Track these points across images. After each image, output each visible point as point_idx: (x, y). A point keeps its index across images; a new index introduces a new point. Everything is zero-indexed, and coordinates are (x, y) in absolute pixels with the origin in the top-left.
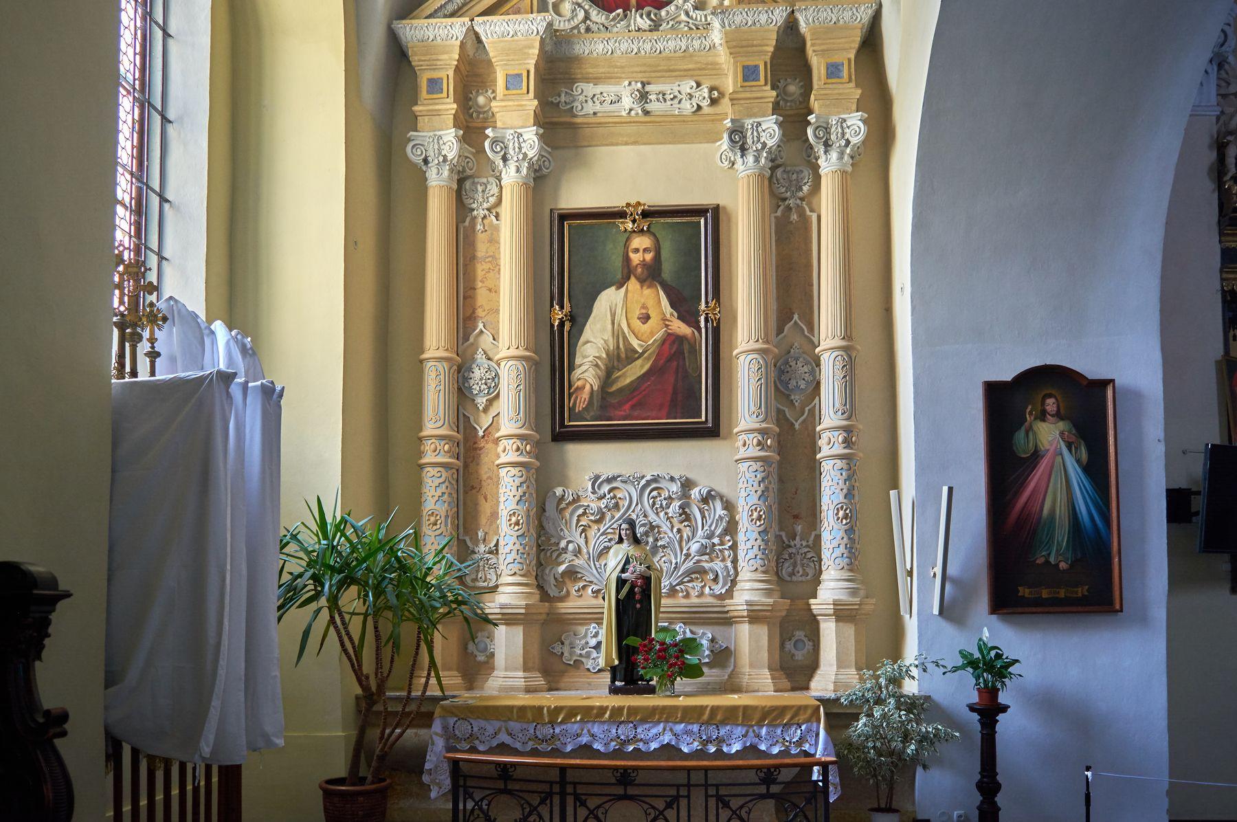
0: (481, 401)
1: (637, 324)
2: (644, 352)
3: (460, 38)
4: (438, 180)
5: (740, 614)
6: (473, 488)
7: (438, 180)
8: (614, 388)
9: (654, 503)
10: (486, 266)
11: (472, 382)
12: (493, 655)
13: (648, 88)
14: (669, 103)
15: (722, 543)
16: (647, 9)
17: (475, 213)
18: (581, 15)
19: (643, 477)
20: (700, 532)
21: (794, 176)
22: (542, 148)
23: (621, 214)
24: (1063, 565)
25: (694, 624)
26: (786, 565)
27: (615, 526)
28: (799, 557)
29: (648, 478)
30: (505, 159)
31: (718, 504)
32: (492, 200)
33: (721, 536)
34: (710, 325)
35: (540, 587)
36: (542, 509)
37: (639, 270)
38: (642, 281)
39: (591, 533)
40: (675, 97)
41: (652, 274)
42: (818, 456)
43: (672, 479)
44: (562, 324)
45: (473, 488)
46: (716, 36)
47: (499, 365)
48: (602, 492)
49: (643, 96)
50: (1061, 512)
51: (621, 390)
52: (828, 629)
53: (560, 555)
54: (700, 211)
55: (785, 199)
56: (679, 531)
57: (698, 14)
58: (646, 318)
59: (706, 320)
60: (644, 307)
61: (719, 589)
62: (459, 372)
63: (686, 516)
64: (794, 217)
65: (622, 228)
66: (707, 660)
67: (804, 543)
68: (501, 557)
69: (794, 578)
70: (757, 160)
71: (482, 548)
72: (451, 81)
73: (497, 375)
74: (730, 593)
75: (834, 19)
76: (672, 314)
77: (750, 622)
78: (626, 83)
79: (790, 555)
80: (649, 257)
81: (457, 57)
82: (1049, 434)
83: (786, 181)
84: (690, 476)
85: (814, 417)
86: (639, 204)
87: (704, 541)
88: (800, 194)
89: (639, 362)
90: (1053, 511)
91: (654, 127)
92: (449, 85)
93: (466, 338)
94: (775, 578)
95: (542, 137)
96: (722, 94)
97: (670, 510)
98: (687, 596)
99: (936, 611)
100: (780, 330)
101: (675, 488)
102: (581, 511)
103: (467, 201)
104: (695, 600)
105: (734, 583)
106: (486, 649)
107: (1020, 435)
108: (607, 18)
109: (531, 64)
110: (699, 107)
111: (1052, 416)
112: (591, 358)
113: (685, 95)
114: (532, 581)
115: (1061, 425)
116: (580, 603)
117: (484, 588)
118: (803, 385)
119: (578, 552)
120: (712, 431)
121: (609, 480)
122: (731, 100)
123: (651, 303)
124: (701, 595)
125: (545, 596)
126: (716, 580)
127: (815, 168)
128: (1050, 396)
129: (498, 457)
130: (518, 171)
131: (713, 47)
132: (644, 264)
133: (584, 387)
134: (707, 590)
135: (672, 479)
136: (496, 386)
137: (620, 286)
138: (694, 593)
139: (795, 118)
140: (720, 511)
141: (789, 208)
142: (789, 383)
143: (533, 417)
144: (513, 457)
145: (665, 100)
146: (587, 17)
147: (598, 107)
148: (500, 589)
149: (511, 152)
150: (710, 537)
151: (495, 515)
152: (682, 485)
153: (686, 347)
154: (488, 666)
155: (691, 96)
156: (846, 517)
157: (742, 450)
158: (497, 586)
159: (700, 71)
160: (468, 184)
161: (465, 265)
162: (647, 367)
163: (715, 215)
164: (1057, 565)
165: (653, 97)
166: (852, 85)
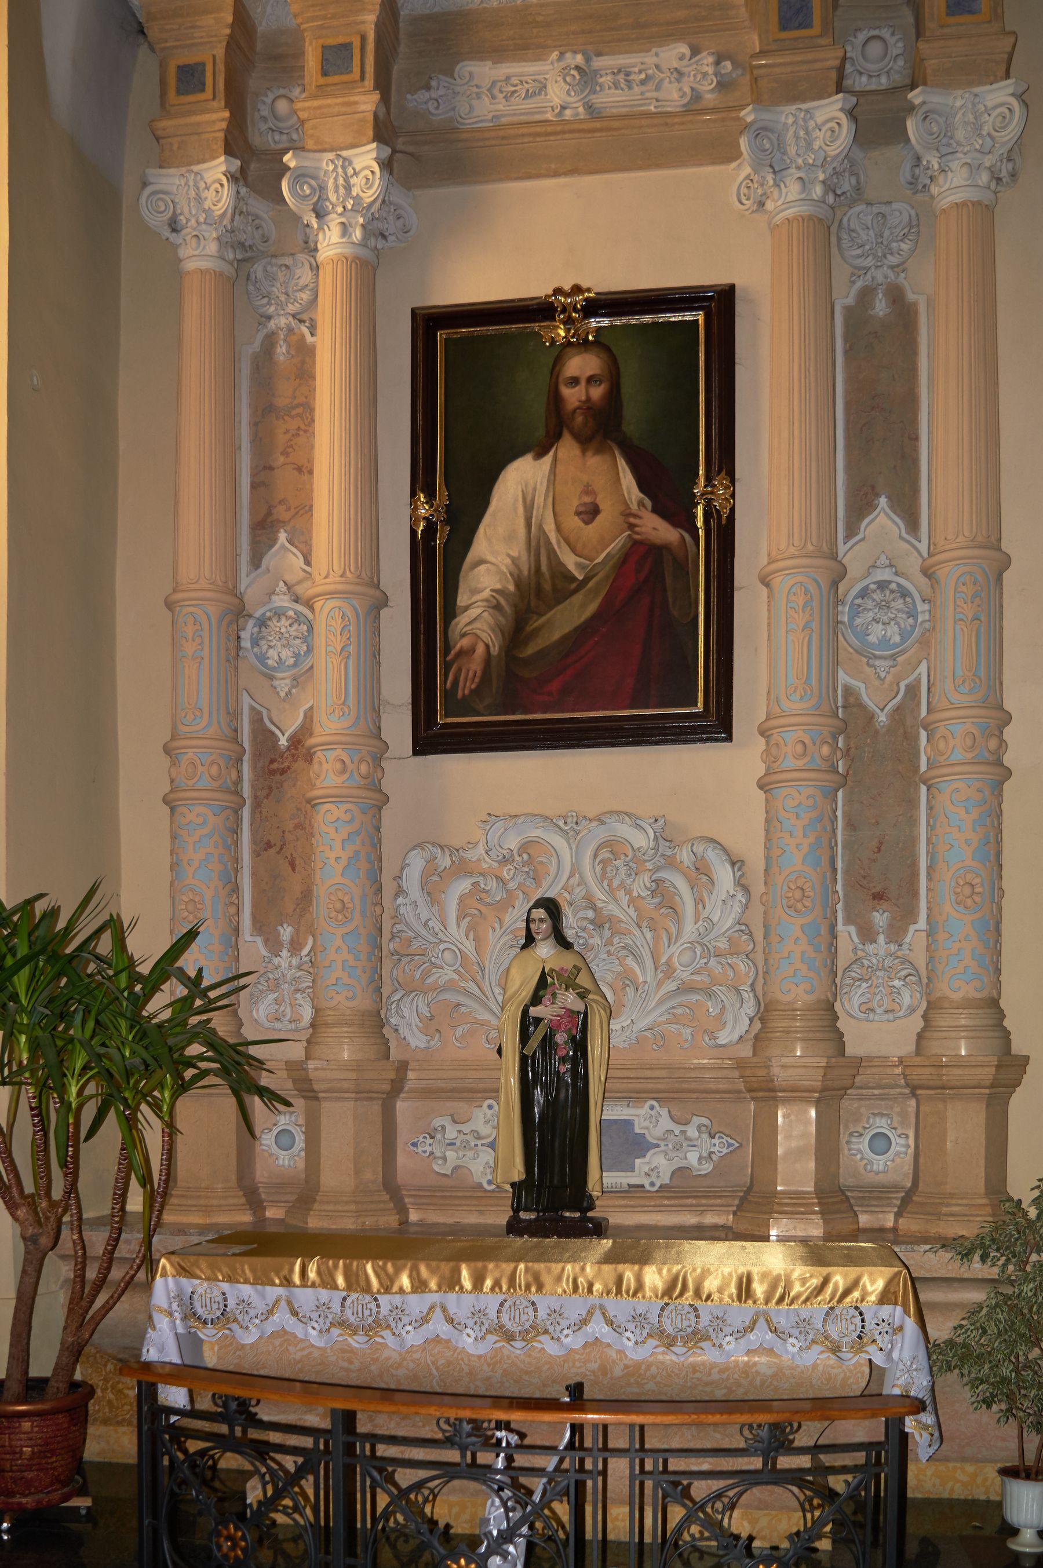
8: (530, 650)
10: (293, 424)
14: (637, 89)
17: (272, 324)
23: (541, 311)
32: (305, 296)
37: (579, 419)
38: (584, 441)
41: (603, 428)
47: (312, 609)
51: (541, 654)
58: (591, 513)
60: (588, 490)
72: (221, 67)
76: (641, 504)
78: (555, 55)
80: (597, 392)
86: (577, 289)
89: (577, 599)
92: (215, 78)
95: (387, 165)
112: (486, 593)
132: (588, 406)
133: (472, 650)
137: (540, 454)
147: (501, 106)
149: (333, 197)
155: (680, 74)
162: (592, 608)
163: (721, 304)
165: (606, 80)
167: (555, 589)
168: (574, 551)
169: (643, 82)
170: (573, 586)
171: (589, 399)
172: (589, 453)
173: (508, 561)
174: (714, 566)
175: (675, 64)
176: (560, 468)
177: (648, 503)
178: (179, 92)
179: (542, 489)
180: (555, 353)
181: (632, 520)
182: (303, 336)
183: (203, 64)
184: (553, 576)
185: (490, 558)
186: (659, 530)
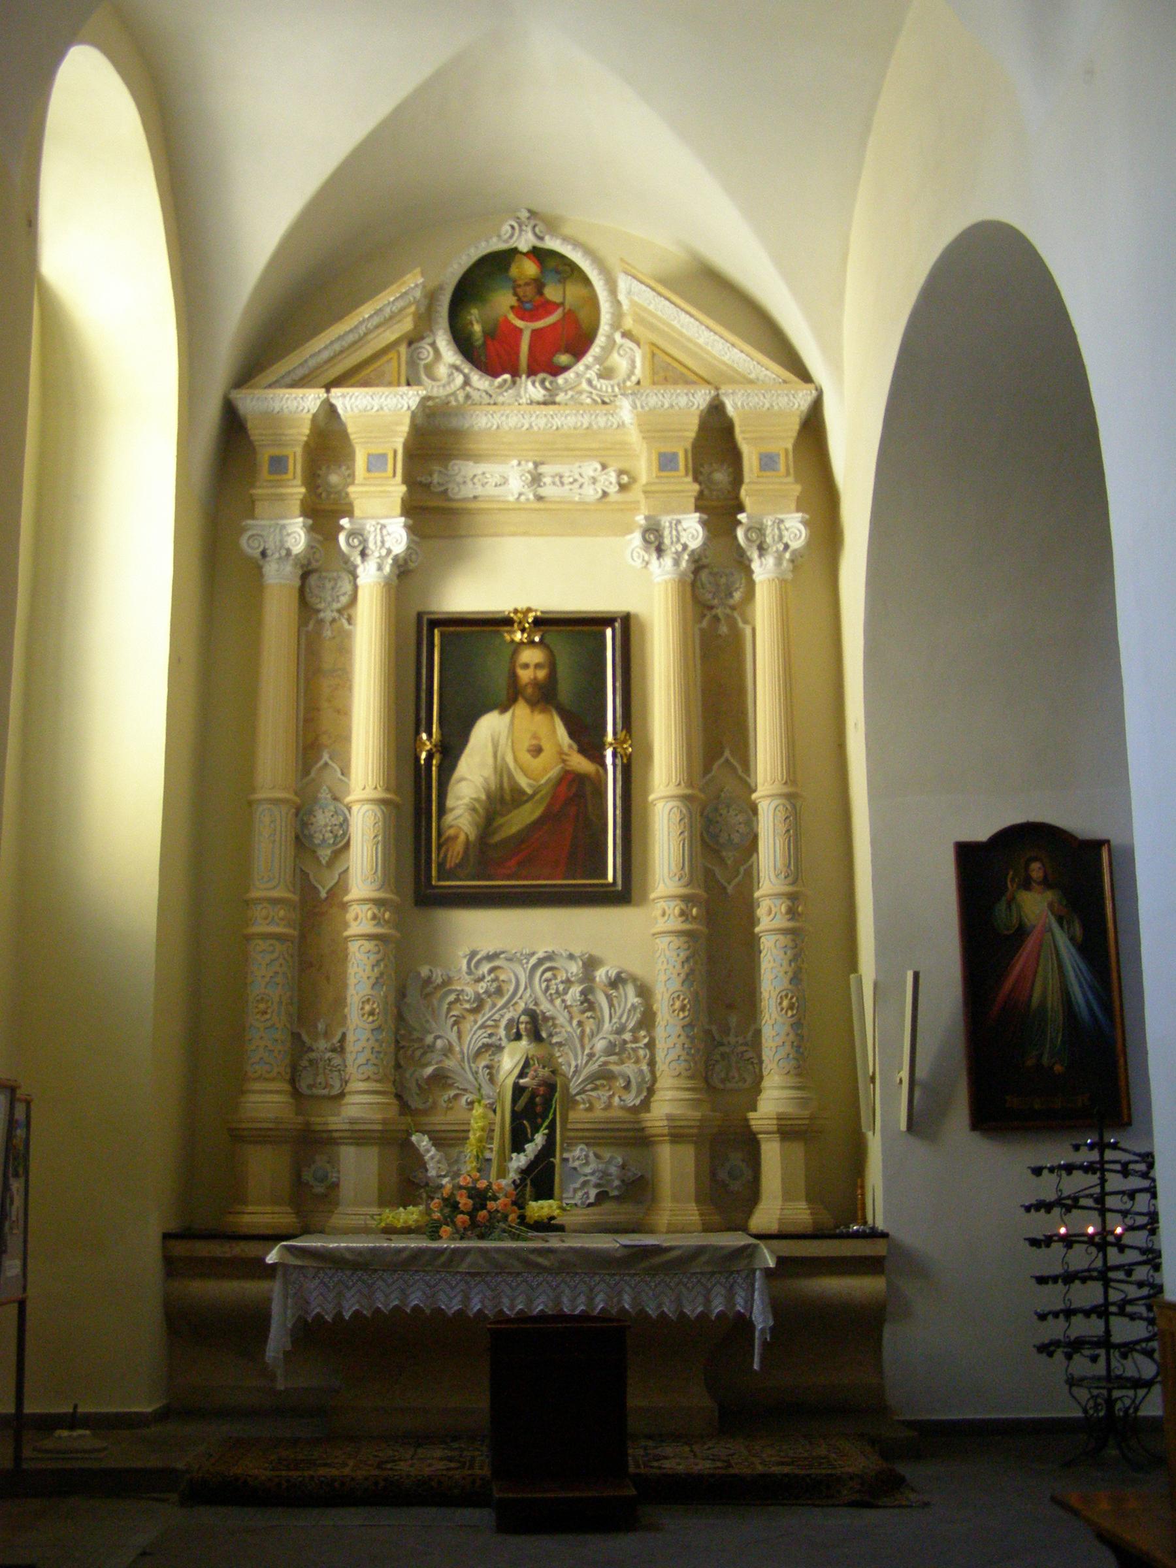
0: (325, 854)
1: (526, 757)
2: (535, 794)
3: (313, 411)
4: (279, 578)
5: (659, 1131)
6: (311, 965)
7: (279, 578)
8: (496, 838)
9: (548, 988)
11: (313, 828)
12: (336, 1186)
13: (542, 469)
14: (567, 487)
15: (635, 1040)
16: (541, 376)
17: (322, 615)
18: (460, 379)
19: (533, 954)
20: (607, 1026)
21: (723, 580)
22: (410, 541)
24: (1058, 1068)
25: (599, 1145)
26: (717, 1068)
27: (496, 1017)
28: (734, 1059)
29: (541, 954)
30: (363, 554)
31: (630, 990)
32: (344, 600)
33: (634, 1031)
34: (618, 761)
35: (399, 1097)
36: (402, 994)
38: (533, 704)
39: (467, 1026)
40: (575, 480)
41: (545, 696)
42: (757, 930)
43: (571, 957)
44: (430, 756)
45: (311, 965)
46: (625, 411)
48: (480, 972)
49: (536, 479)
50: (1054, 1001)
52: (771, 1153)
53: (424, 1054)
54: (606, 620)
55: (711, 608)
56: (580, 1024)
57: (603, 384)
58: (537, 751)
59: (614, 755)
60: (535, 736)
61: (632, 1099)
62: (297, 814)
63: (588, 1003)
64: (724, 629)
65: (508, 637)
66: (615, 1193)
67: (741, 1040)
68: (350, 1058)
69: (729, 1085)
70: (677, 563)
71: (322, 1044)
73: (346, 820)
74: (645, 1105)
75: (767, 405)
76: (570, 747)
77: (672, 1142)
78: (515, 462)
79: (723, 1055)
80: (541, 674)
81: (307, 432)
82: (1035, 906)
83: (712, 590)
84: (596, 952)
85: (750, 880)
86: (529, 610)
87: (612, 1038)
88: (731, 602)
89: (528, 806)
90: (1043, 1003)
91: (548, 515)
93: (306, 771)
94: (703, 1085)
96: (633, 479)
97: (568, 997)
98: (591, 1109)
99: (903, 1126)
100: (707, 769)
101: (575, 968)
102: (452, 997)
103: (313, 600)
104: (598, 1114)
105: (651, 1091)
106: (323, 1179)
107: (1002, 906)
108: (491, 385)
109: (399, 443)
110: (605, 494)
111: (1039, 883)
112: (466, 800)
113: (588, 479)
114: (389, 1088)
115: (1050, 895)
116: (450, 1117)
117: (324, 1097)
118: (736, 838)
119: (448, 1051)
120: (623, 895)
121: (490, 958)
122: (645, 492)
123: (543, 732)
124: (609, 1106)
125: (405, 1107)
126: (627, 1087)
127: (749, 572)
128: (1036, 859)
129: (346, 925)
130: (380, 568)
131: (621, 425)
132: (535, 683)
133: (456, 837)
134: (616, 1100)
135: (571, 957)
136: (344, 834)
137: (504, 709)
138: (599, 1105)
139: (721, 510)
140: (633, 999)
141: (716, 619)
142: (718, 835)
143: (391, 874)
144: (368, 927)
145: (562, 484)
146: (467, 382)
148: (349, 1099)
150: (620, 1031)
151: (340, 1002)
152: (584, 964)
153: (588, 788)
154: (329, 1196)
156: (791, 1007)
157: (661, 920)
158: (342, 1095)
159: (605, 451)
160: (313, 580)
161: (307, 680)
162: (538, 813)
163: (626, 626)
164: (1051, 1068)
165: (547, 480)
166: (791, 479)
167: (513, 800)
168: (526, 774)
169: (571, 483)
170: (525, 798)
171: (535, 678)
172: (536, 713)
173: (481, 780)
174: (619, 791)
175: (592, 474)
176: (516, 721)
177: (575, 746)
178: (270, 473)
179: (504, 733)
180: (512, 648)
181: (565, 757)
182: (342, 625)
183: (287, 457)
184: (512, 790)
185: (468, 776)
186: (581, 764)
